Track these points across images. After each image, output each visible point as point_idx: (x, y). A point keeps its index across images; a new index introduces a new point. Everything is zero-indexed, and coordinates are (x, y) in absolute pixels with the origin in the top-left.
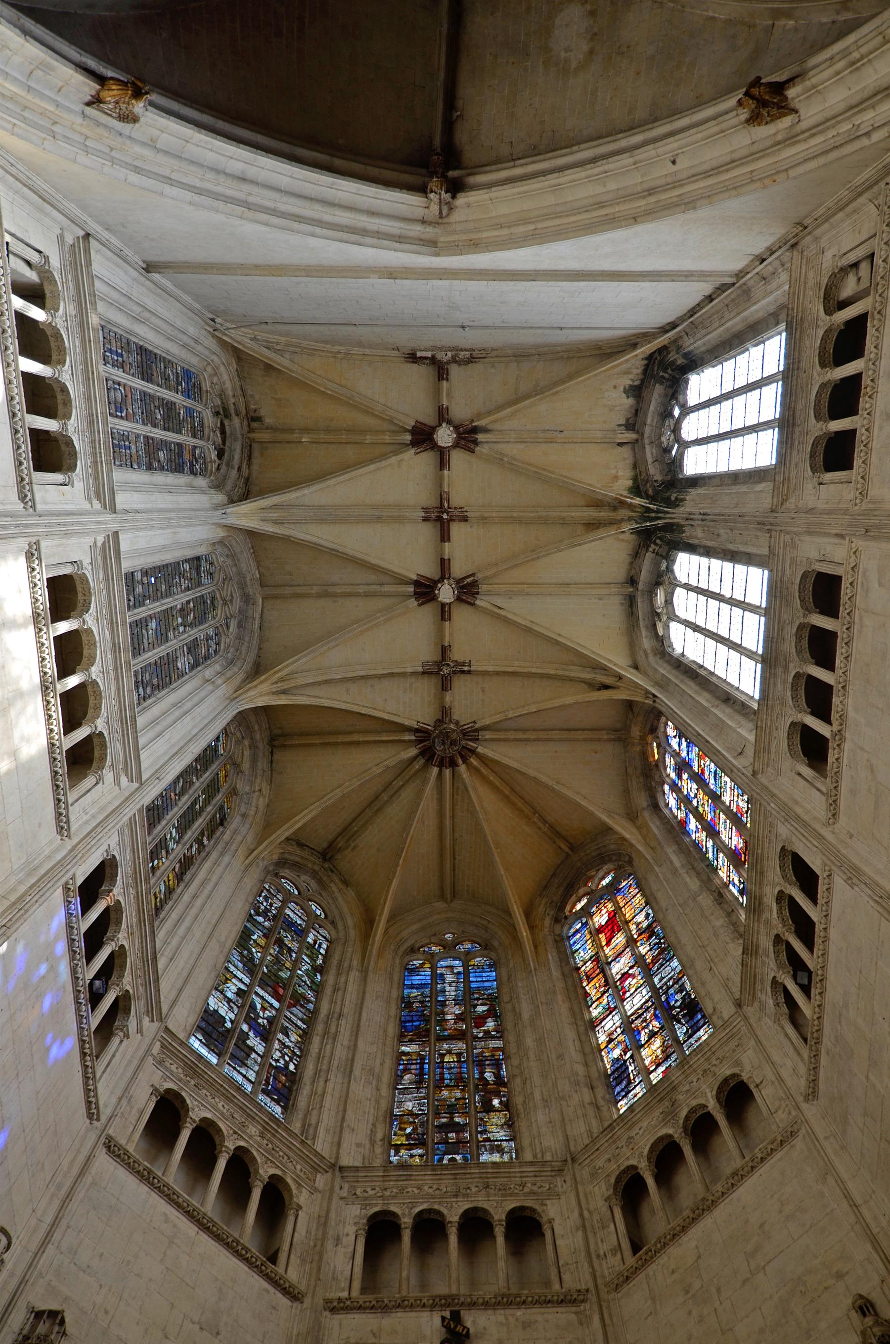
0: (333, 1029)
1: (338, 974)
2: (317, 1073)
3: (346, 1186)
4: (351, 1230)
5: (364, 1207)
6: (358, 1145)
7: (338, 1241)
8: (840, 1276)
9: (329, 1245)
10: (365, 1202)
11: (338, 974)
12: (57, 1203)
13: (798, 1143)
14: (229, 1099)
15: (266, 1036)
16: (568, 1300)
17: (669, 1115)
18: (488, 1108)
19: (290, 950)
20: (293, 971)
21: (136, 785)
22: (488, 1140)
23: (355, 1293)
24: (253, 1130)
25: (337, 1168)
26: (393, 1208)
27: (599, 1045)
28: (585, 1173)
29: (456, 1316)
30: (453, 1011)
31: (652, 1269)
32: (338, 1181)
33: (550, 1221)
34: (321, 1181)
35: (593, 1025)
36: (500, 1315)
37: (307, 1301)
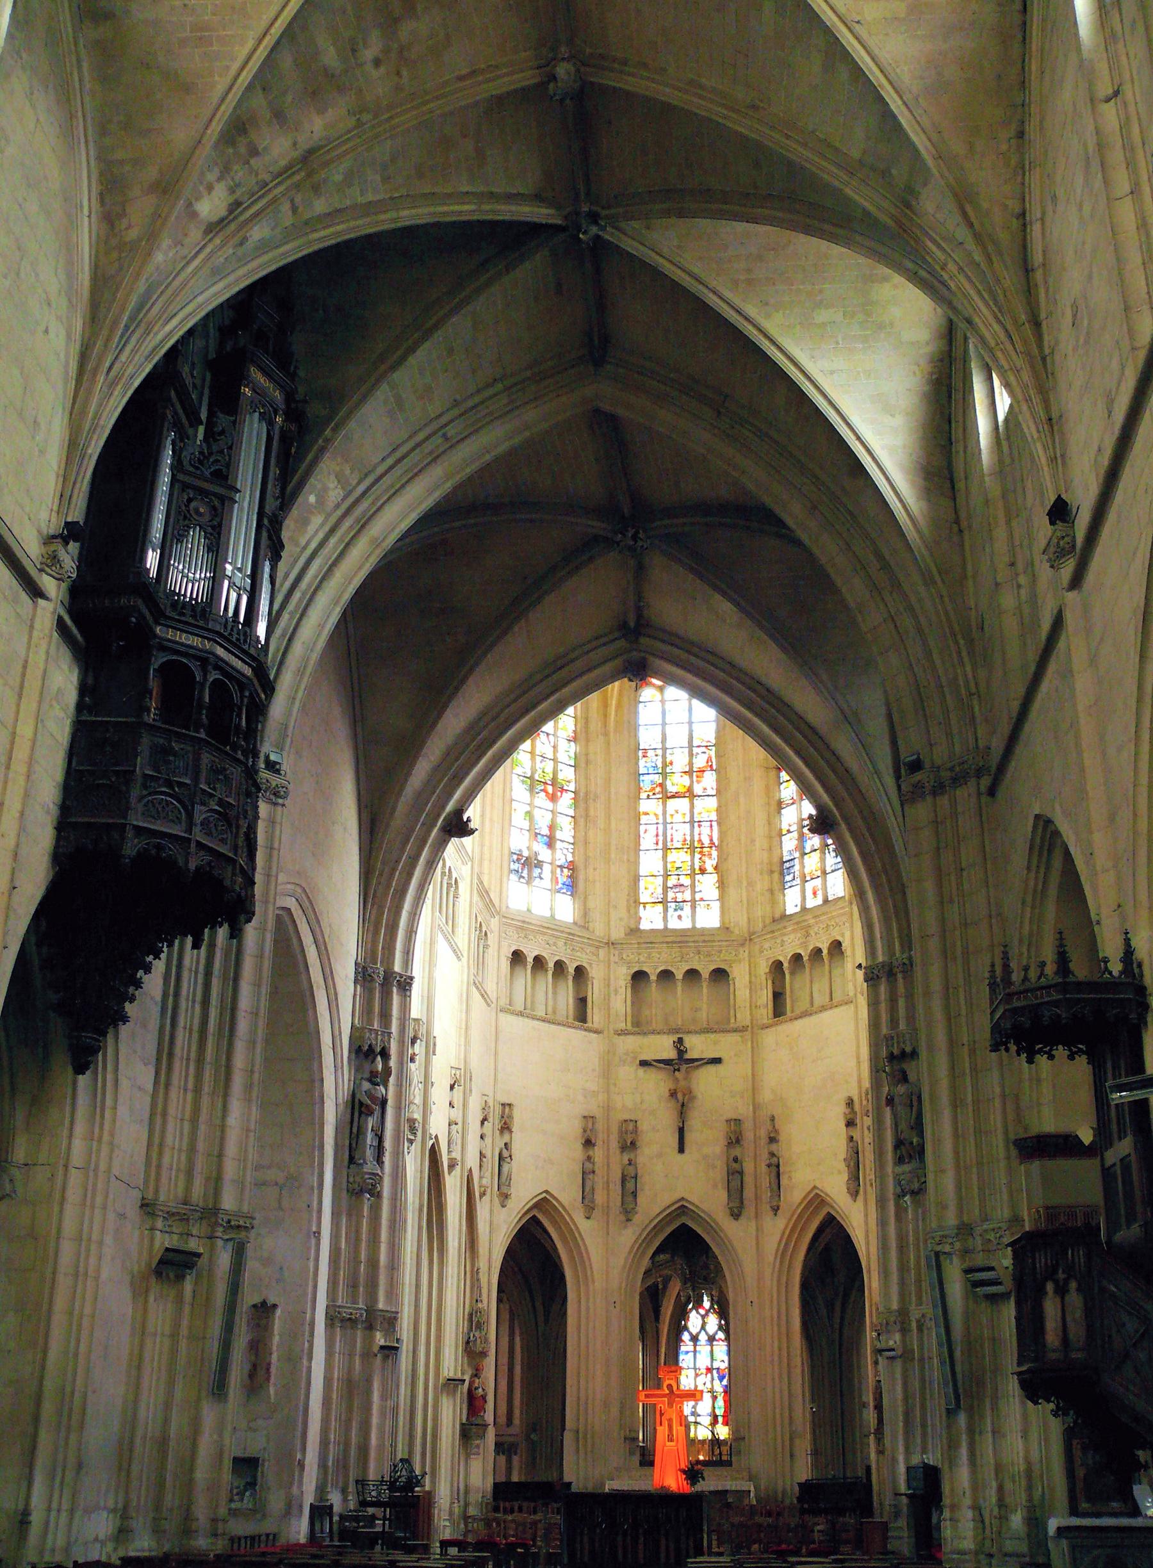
0: (592, 812)
1: (588, 740)
2: (587, 859)
3: (617, 953)
4: (622, 983)
5: (629, 968)
6: (621, 919)
7: (616, 991)
8: (847, 1082)
9: (612, 995)
10: (629, 964)
11: (588, 740)
12: (492, 1057)
13: (852, 1006)
14: (544, 934)
15: (551, 843)
16: (735, 1030)
17: (804, 944)
18: (703, 871)
19: (548, 734)
20: (555, 760)
21: (470, 863)
22: (702, 900)
23: (629, 1024)
24: (561, 943)
25: (610, 944)
26: (644, 969)
27: (781, 829)
28: (757, 947)
29: (680, 1040)
30: (680, 761)
31: (779, 1028)
32: (612, 951)
33: (733, 979)
34: (602, 952)
35: (780, 806)
36: (702, 1037)
37: (606, 1032)
